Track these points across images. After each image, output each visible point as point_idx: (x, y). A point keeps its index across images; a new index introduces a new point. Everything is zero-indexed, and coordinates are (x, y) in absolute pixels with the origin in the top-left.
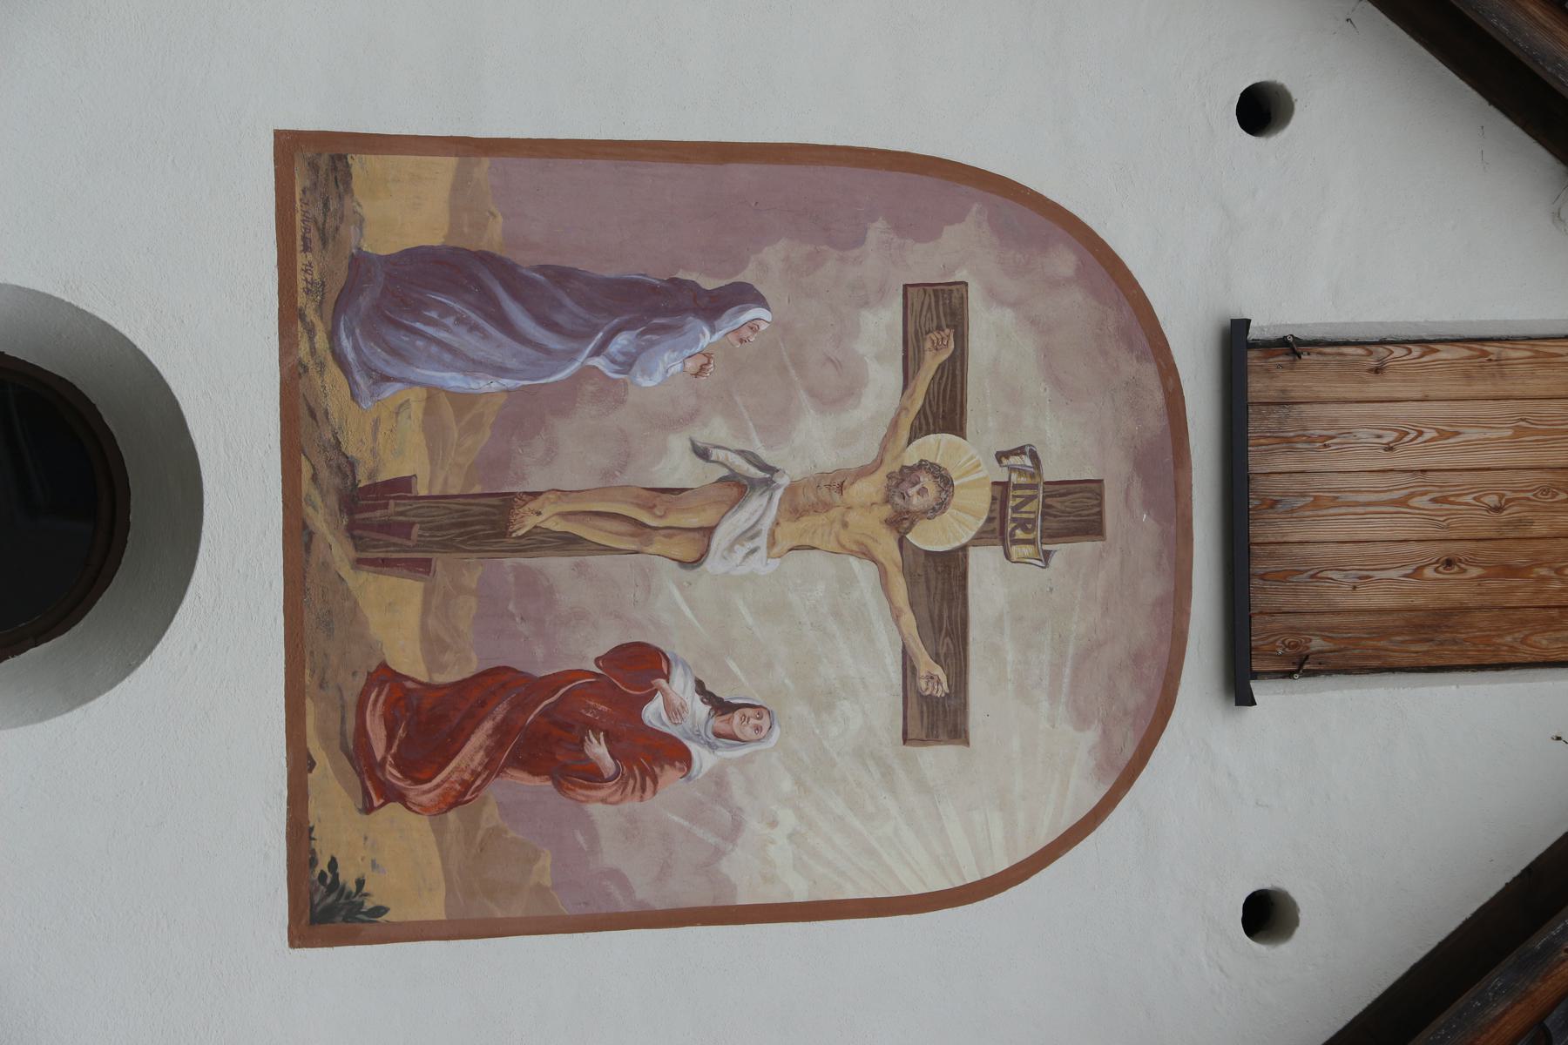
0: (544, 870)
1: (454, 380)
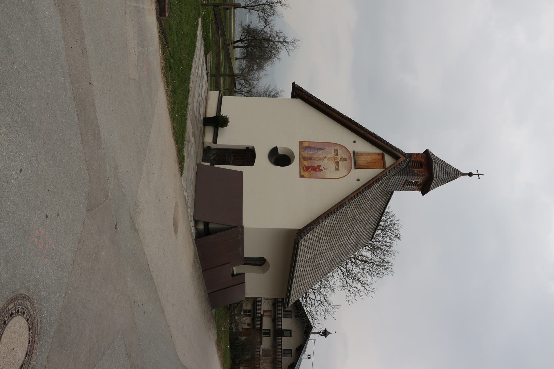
0: (314, 175)
1: (309, 152)
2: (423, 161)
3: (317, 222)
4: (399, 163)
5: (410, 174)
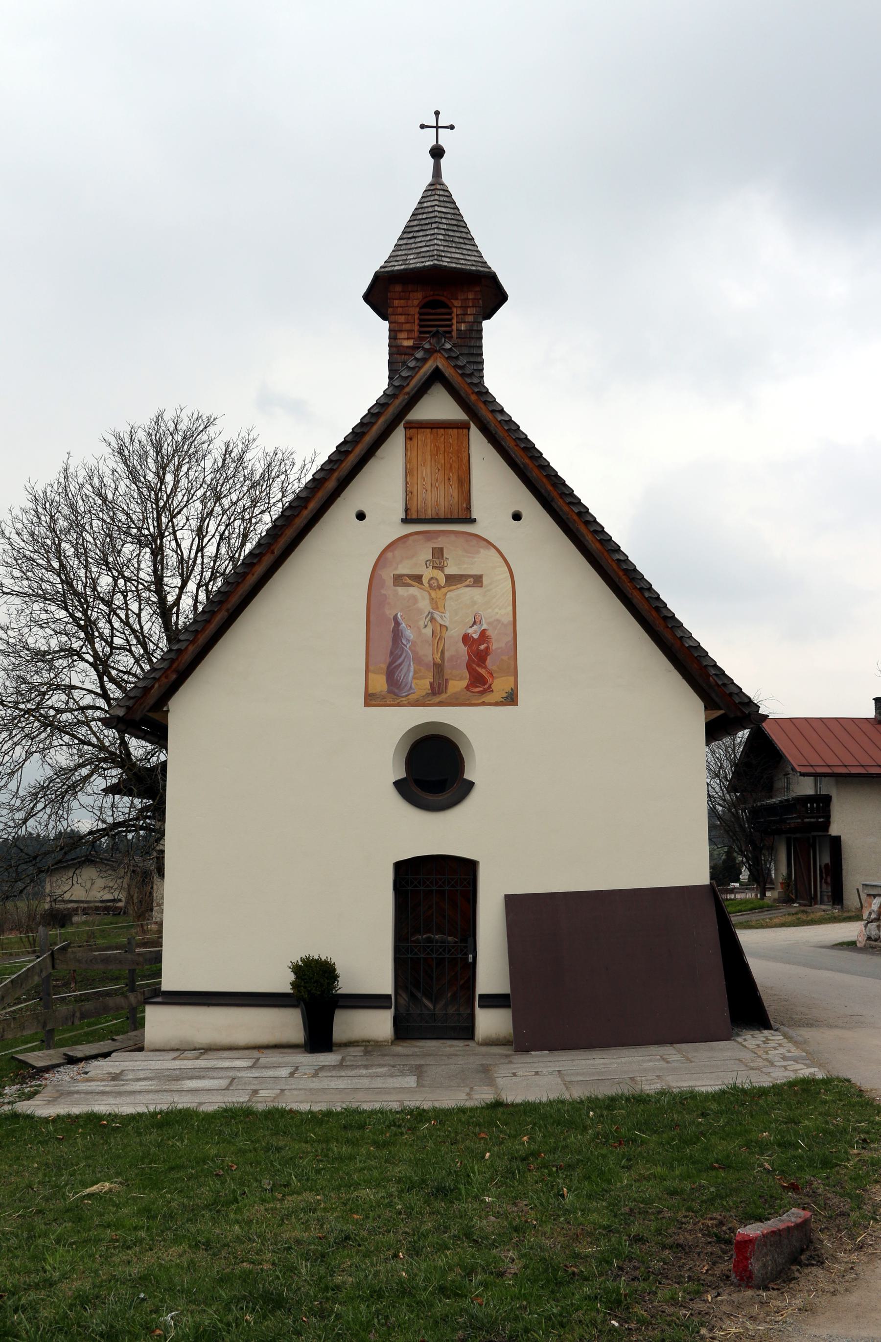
0: (505, 658)
1: (411, 674)
2: (419, 295)
3: (696, 655)
4: (463, 375)
5: (473, 347)
